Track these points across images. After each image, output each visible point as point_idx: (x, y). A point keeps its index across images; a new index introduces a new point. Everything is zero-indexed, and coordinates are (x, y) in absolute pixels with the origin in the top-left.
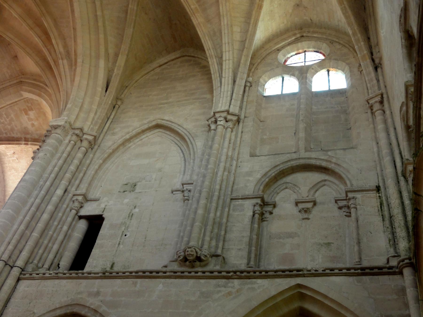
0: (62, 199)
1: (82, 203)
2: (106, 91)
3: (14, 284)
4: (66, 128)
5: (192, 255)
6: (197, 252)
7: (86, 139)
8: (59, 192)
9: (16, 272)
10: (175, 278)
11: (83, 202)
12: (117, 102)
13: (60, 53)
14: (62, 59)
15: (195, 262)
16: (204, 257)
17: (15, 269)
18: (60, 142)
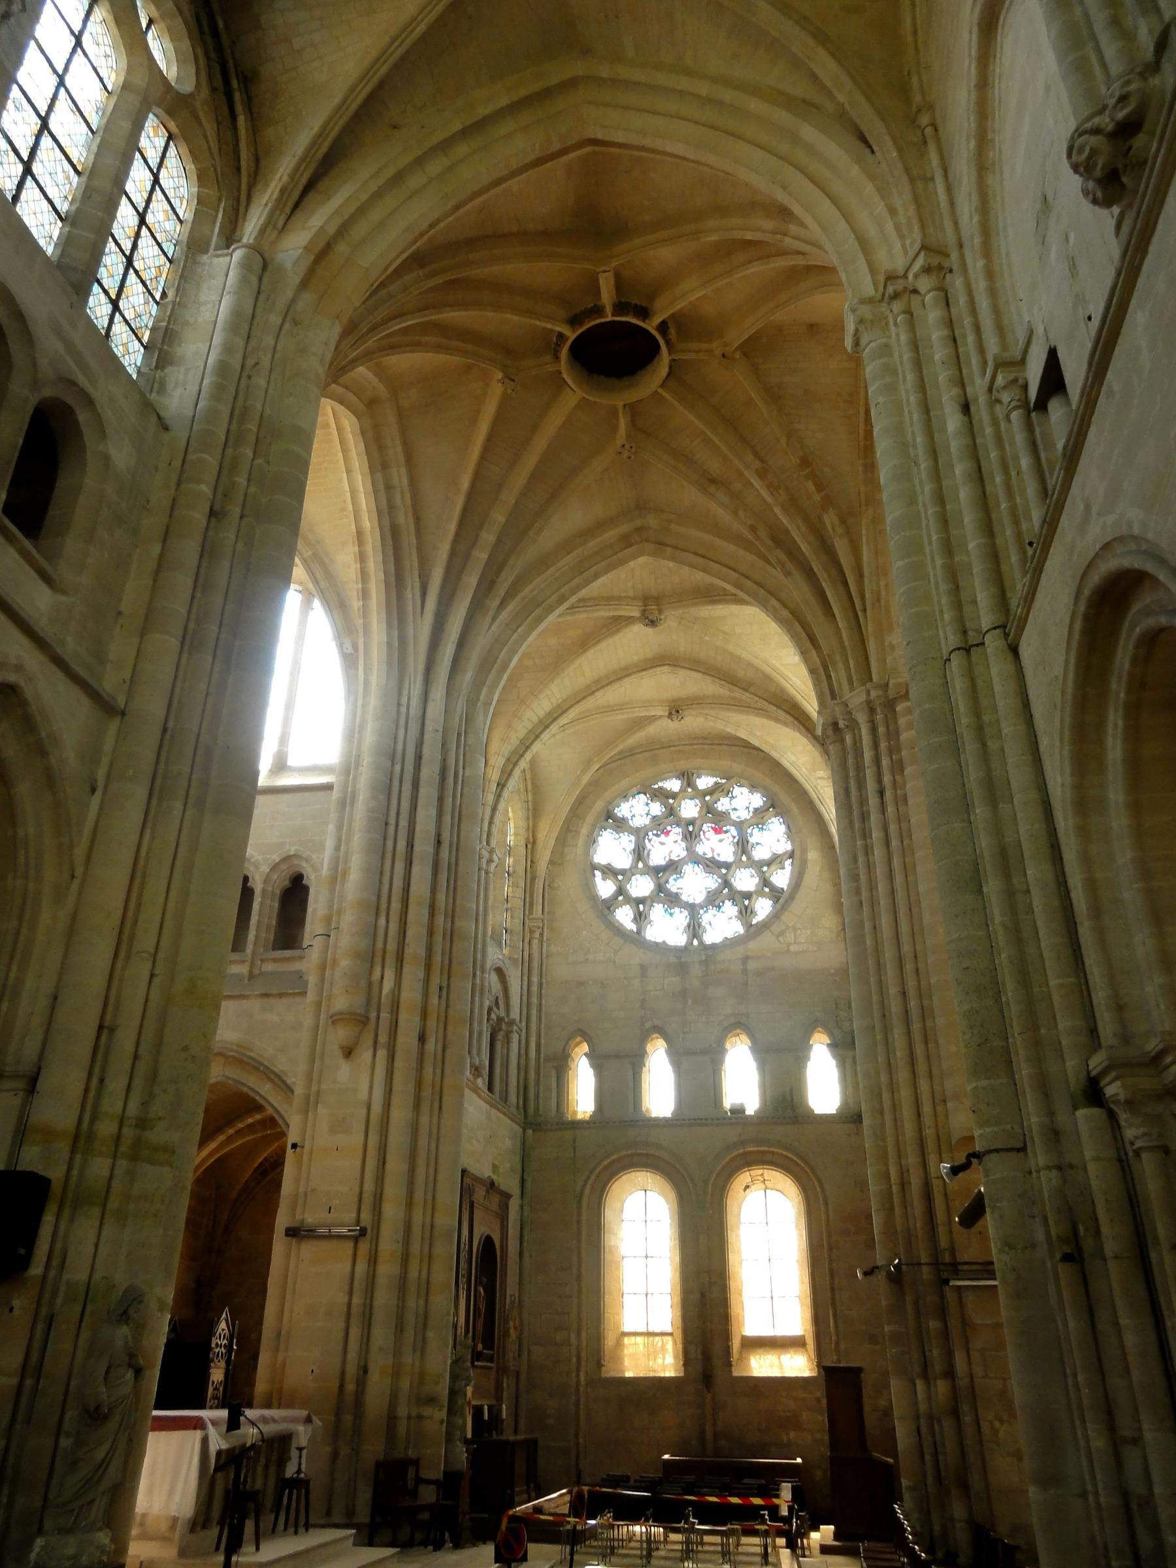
0: (970, 429)
1: (1015, 381)
2: (873, 152)
3: (1010, 667)
4: (869, 316)
5: (1094, 152)
6: (1096, 131)
7: (916, 276)
8: (953, 422)
9: (993, 642)
10: (1145, 252)
11: (1012, 376)
12: (919, 127)
13: (774, 232)
14: (785, 234)
15: (1130, 148)
16: (1122, 109)
17: (988, 639)
18: (886, 350)
